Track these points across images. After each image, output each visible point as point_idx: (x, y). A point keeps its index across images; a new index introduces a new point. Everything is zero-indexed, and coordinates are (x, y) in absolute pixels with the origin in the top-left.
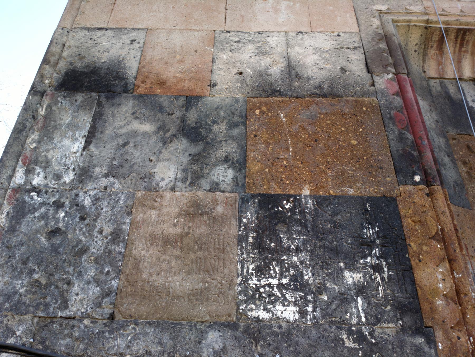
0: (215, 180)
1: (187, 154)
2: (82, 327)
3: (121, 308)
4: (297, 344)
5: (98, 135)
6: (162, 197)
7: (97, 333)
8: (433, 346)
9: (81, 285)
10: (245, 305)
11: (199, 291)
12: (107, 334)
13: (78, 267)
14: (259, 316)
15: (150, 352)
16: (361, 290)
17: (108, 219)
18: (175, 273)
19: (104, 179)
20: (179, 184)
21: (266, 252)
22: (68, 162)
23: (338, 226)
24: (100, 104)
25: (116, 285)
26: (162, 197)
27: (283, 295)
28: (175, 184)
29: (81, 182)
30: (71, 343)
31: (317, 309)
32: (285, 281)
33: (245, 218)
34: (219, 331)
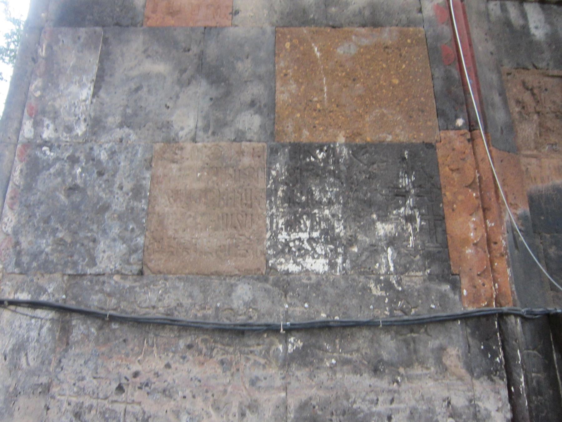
0: (241, 128)
1: (208, 98)
2: (113, 283)
3: (150, 265)
4: (325, 293)
5: (107, 79)
6: (182, 149)
7: (128, 288)
8: (457, 292)
9: (107, 243)
10: (274, 259)
11: (227, 247)
12: (137, 289)
13: (102, 224)
14: (288, 269)
15: (181, 304)
16: (391, 241)
17: (127, 174)
18: (201, 229)
19: (118, 130)
20: (201, 133)
21: (297, 206)
22: (78, 111)
23: (372, 177)
24: (106, 41)
25: (142, 242)
26: (182, 149)
27: (314, 249)
28: (195, 134)
29: (94, 134)
31: (347, 261)
32: (315, 235)
33: (274, 170)
34: (249, 284)
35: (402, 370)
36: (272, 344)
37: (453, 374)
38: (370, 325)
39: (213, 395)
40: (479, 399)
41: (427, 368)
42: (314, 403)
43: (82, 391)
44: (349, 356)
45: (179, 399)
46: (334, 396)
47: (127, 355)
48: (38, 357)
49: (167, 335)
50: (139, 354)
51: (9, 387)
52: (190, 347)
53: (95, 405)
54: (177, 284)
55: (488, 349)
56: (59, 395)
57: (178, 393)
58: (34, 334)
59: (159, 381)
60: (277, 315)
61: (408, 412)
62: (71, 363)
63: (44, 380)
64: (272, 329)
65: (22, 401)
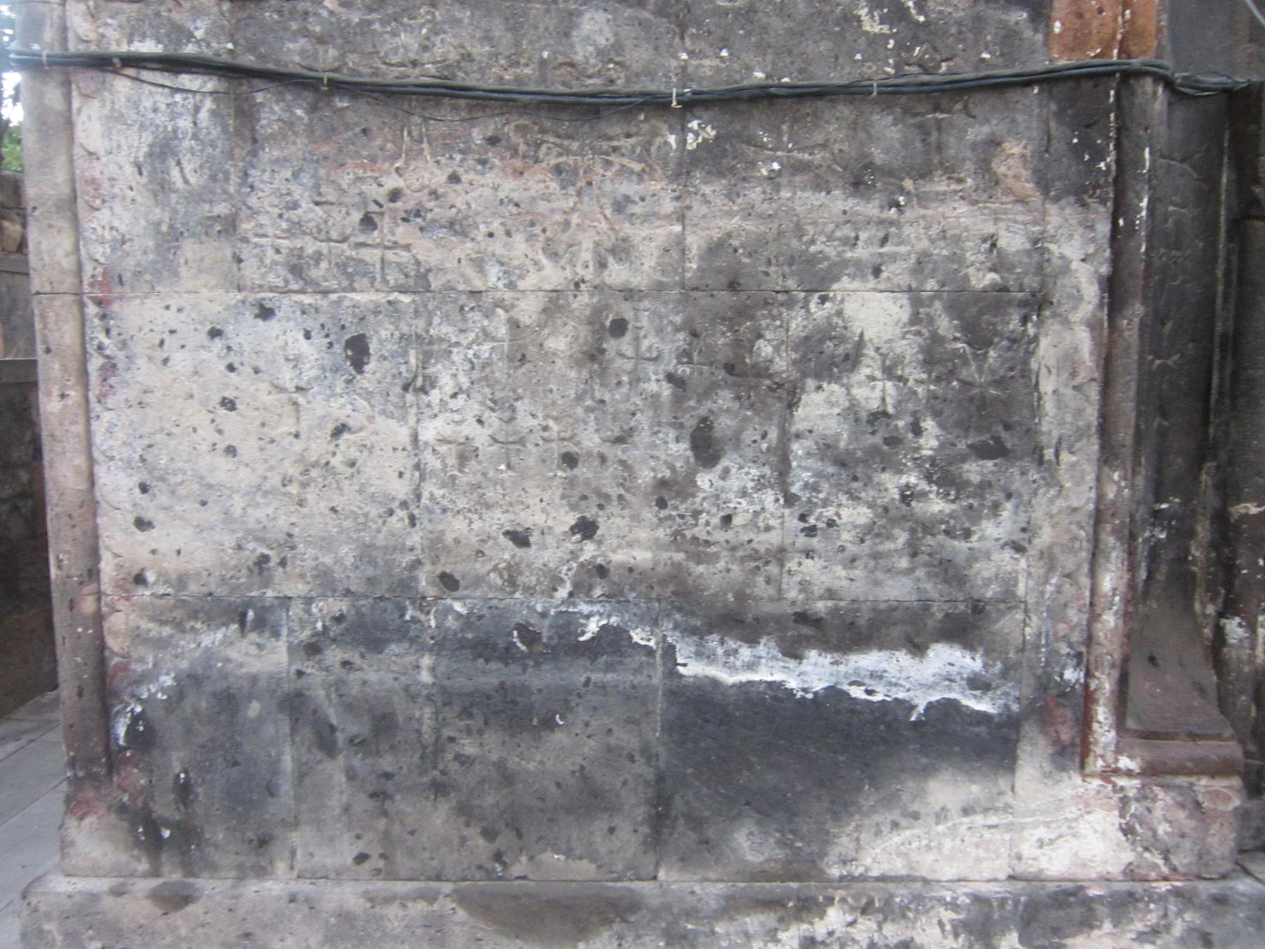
2: (325, 14)
4: (765, 29)
7: (358, 24)
8: (1042, 27)
12: (377, 26)
15: (469, 55)
30: (309, 47)
34: (606, 10)
35: (908, 184)
36: (655, 133)
37: (1009, 191)
38: (853, 92)
39: (544, 231)
40: (1053, 239)
41: (960, 181)
42: (735, 243)
43: (296, 228)
44: (806, 156)
45: (480, 238)
46: (774, 231)
47: (373, 160)
48: (201, 167)
49: (447, 119)
50: (396, 157)
51: (159, 224)
52: (493, 141)
53: (325, 251)
54: (458, 15)
55: (1086, 144)
56: (257, 235)
57: (477, 228)
58: (184, 123)
59: (440, 207)
60: (665, 75)
61: (913, 260)
62: (266, 177)
63: (222, 209)
64: (656, 104)
65: (189, 248)
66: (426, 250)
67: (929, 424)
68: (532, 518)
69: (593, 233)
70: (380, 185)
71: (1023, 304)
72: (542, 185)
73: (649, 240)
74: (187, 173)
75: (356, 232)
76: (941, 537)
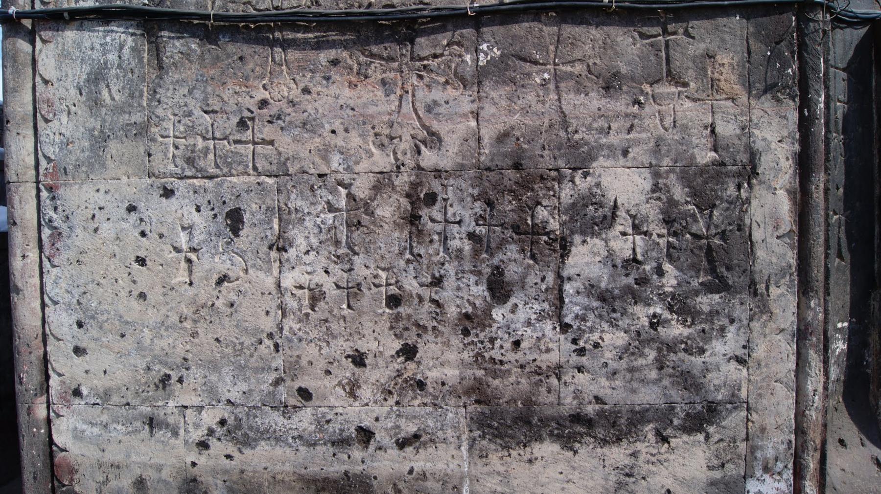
35: (647, 88)
39: (373, 128)
40: (757, 126)
41: (685, 85)
42: (517, 133)
43: (191, 130)
44: (568, 68)
45: (325, 134)
46: (546, 124)
47: (247, 78)
48: (123, 88)
51: (94, 129)
52: (335, 62)
55: (777, 55)
56: (162, 136)
57: (323, 127)
58: (112, 57)
61: (652, 143)
62: (169, 94)
63: (137, 117)
65: (114, 147)
66: (285, 143)
67: (667, 267)
68: (367, 345)
69: (410, 129)
70: (251, 97)
71: (739, 174)
72: (371, 94)
73: (454, 133)
74: (113, 93)
75: (234, 132)
76: (681, 355)
